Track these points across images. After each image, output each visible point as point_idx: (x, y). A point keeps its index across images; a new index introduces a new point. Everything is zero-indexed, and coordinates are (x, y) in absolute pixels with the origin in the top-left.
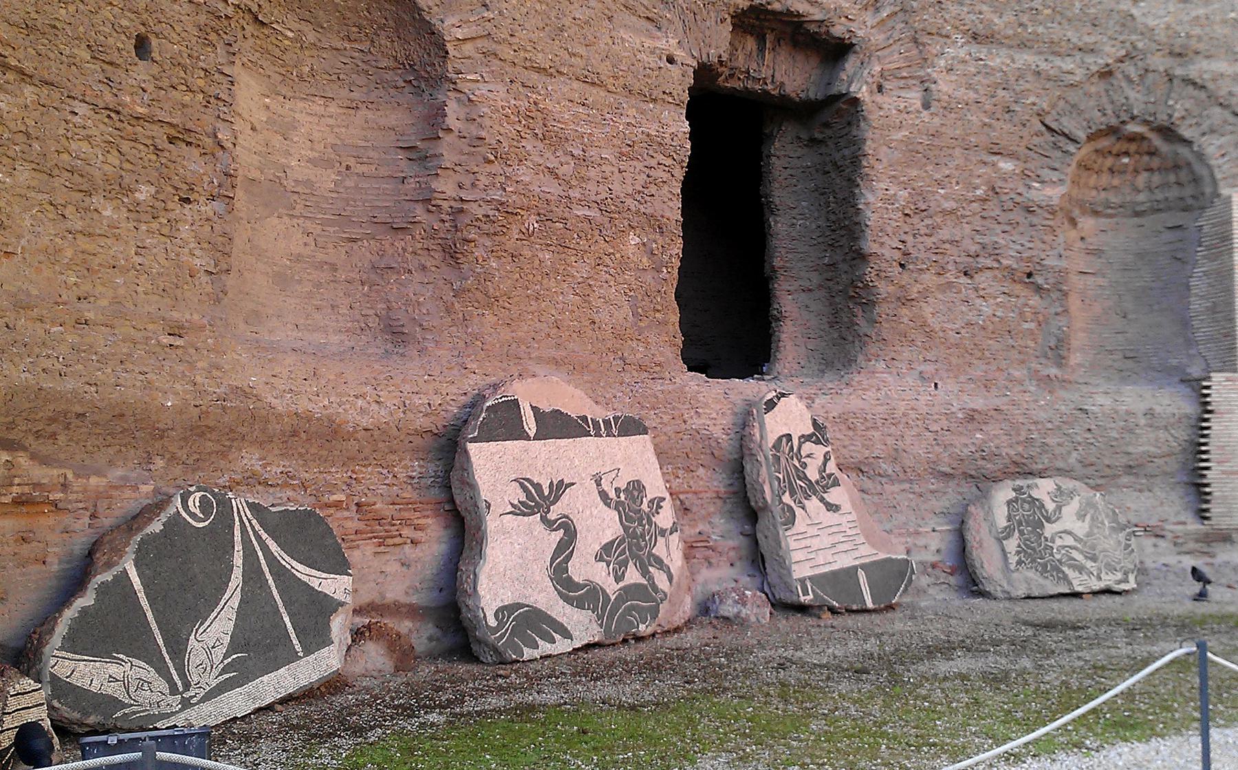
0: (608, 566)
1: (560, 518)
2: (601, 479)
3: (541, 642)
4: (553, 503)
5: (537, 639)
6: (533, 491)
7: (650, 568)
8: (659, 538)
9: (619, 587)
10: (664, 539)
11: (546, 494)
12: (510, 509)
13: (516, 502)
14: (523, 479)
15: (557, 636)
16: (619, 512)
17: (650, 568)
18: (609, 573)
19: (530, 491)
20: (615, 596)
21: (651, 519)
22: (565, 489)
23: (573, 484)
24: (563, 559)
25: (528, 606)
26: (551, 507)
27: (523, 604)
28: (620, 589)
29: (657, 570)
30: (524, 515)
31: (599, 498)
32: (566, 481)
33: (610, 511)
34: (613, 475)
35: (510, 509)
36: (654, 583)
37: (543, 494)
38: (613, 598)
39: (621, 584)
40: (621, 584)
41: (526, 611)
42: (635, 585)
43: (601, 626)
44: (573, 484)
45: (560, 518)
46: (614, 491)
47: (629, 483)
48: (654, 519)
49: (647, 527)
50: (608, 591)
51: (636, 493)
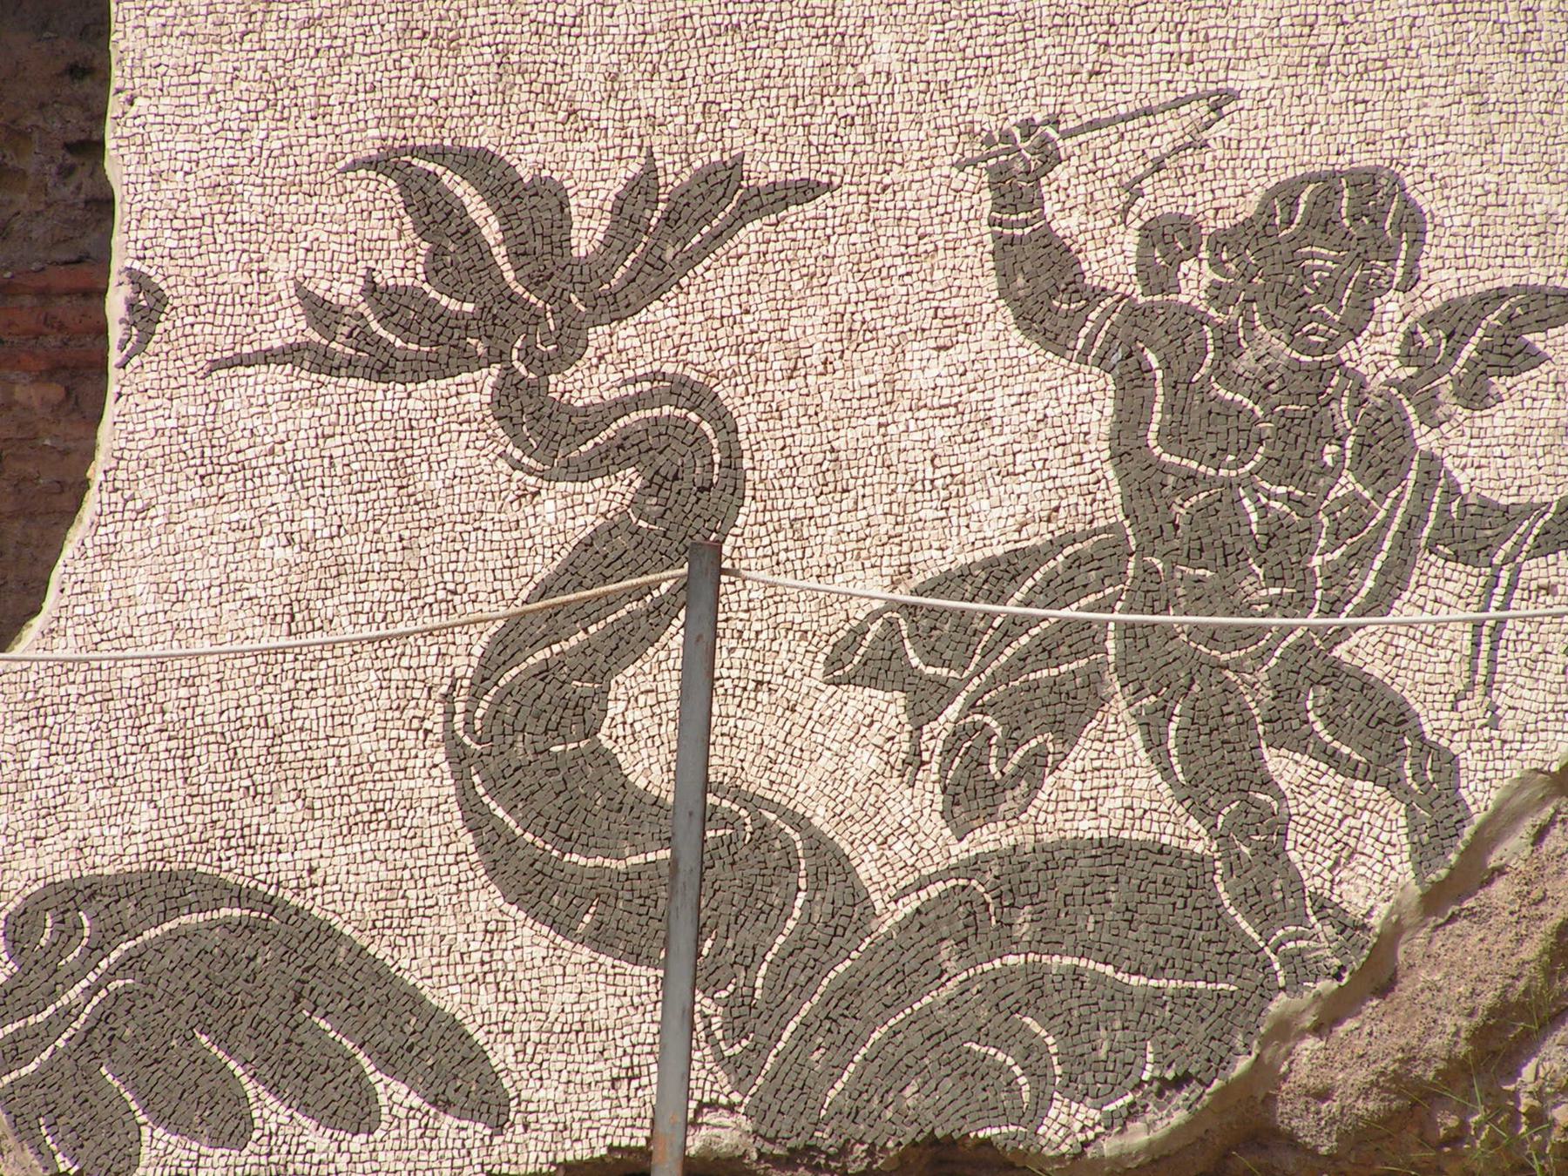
0: (920, 715)
1: (639, 402)
2: (1050, 158)
3: (270, 1111)
4: (617, 307)
5: (250, 1089)
6: (491, 231)
7: (1284, 766)
8: (1430, 566)
9: (960, 850)
10: (1462, 578)
11: (586, 237)
12: (290, 326)
13: (346, 292)
14: (437, 154)
15: (393, 1094)
16: (1132, 381)
17: (1284, 766)
18: (915, 760)
19: (468, 233)
20: (912, 903)
21: (1405, 435)
22: (739, 220)
23: (807, 190)
24: (583, 650)
25: (240, 896)
26: (597, 336)
27: (218, 884)
28: (974, 866)
29: (1335, 780)
30: (383, 369)
31: (992, 282)
32: (764, 168)
33: (1056, 367)
34: (1170, 129)
35: (290, 326)
36: (1274, 854)
37: (564, 244)
38: (891, 915)
39: (989, 838)
40: (989, 838)
41: (225, 924)
42: (1111, 849)
43: (740, 1070)
44: (807, 190)
45: (639, 402)
46: (1131, 241)
47: (1287, 193)
48: (1426, 439)
49: (1348, 483)
50: (866, 871)
51: (1322, 260)
